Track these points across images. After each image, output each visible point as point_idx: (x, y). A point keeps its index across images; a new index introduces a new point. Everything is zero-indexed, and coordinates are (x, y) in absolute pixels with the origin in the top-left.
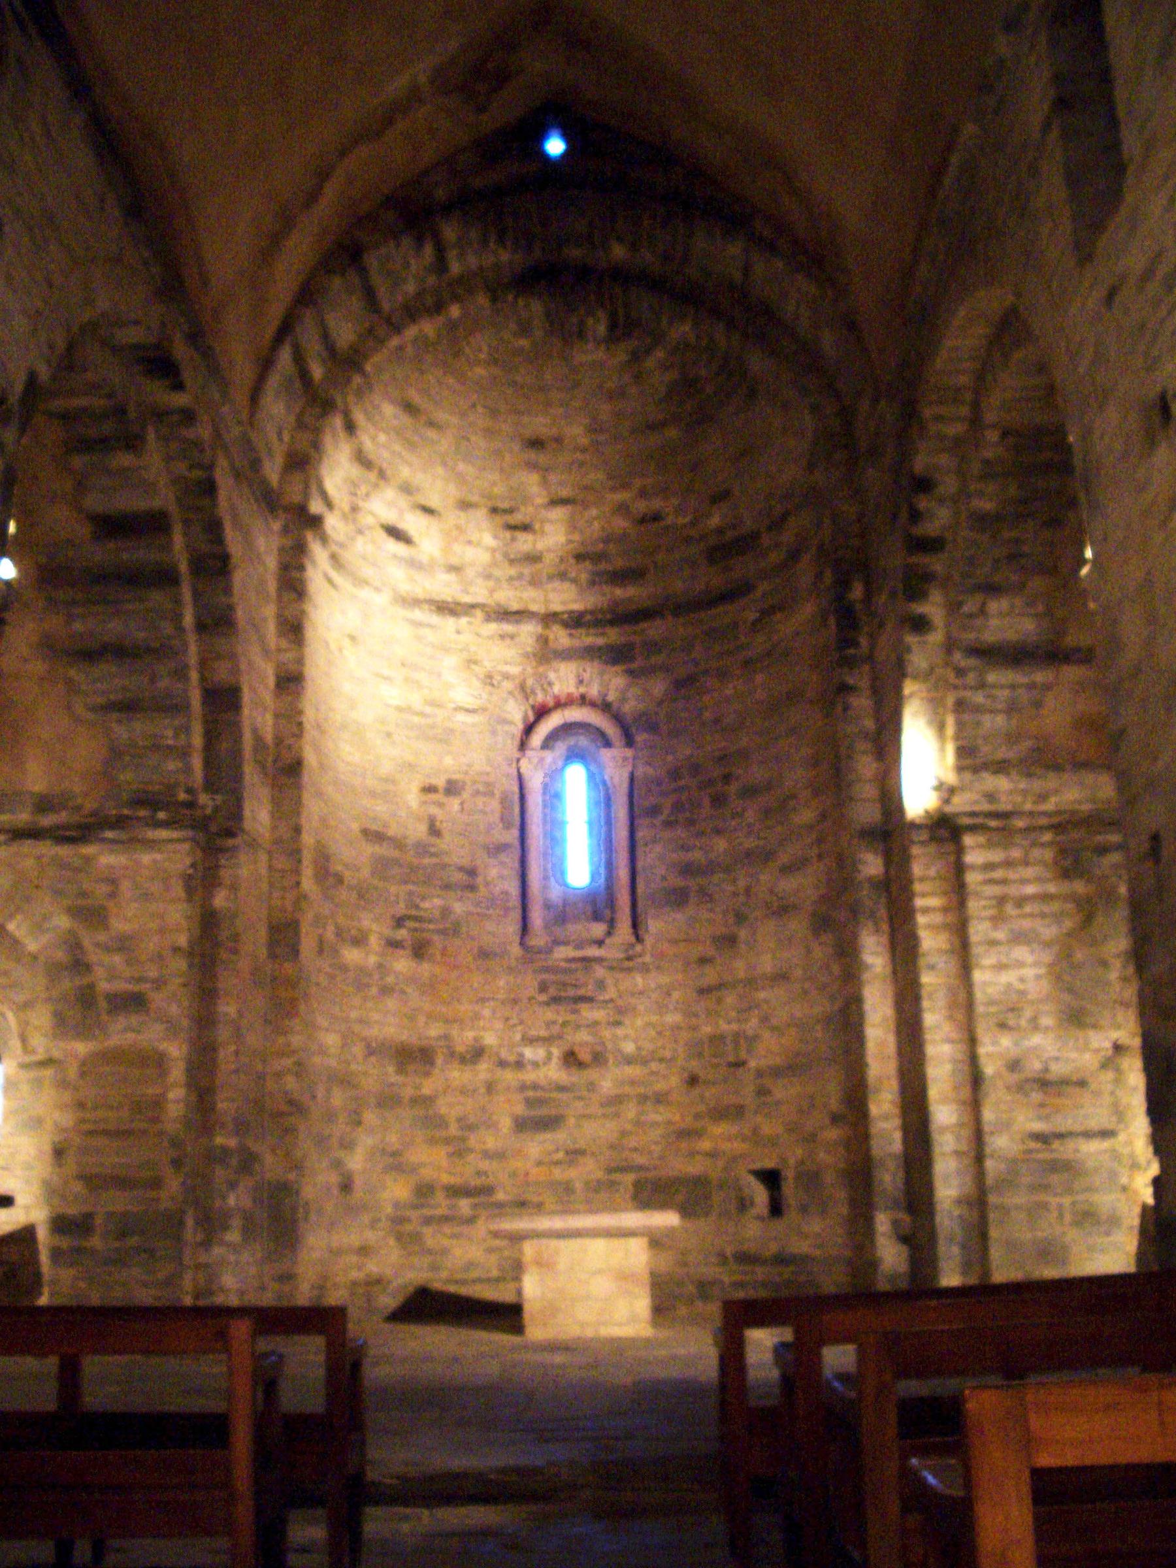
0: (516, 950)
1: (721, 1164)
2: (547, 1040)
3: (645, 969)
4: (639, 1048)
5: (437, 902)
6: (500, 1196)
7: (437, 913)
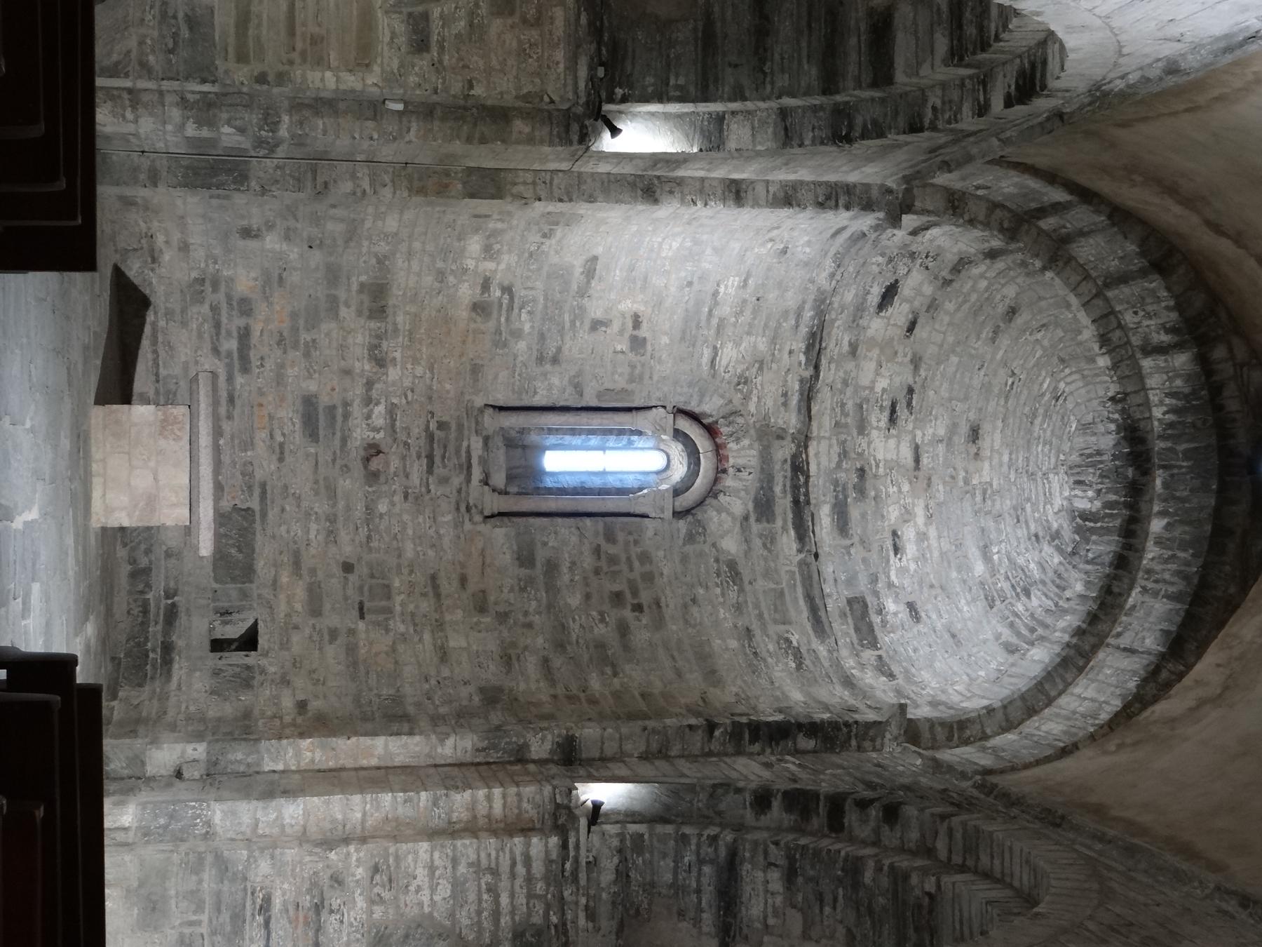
0: (479, 401)
1: (267, 593)
3: (458, 524)
4: (381, 516)
5: (527, 327)
6: (240, 380)
7: (517, 325)
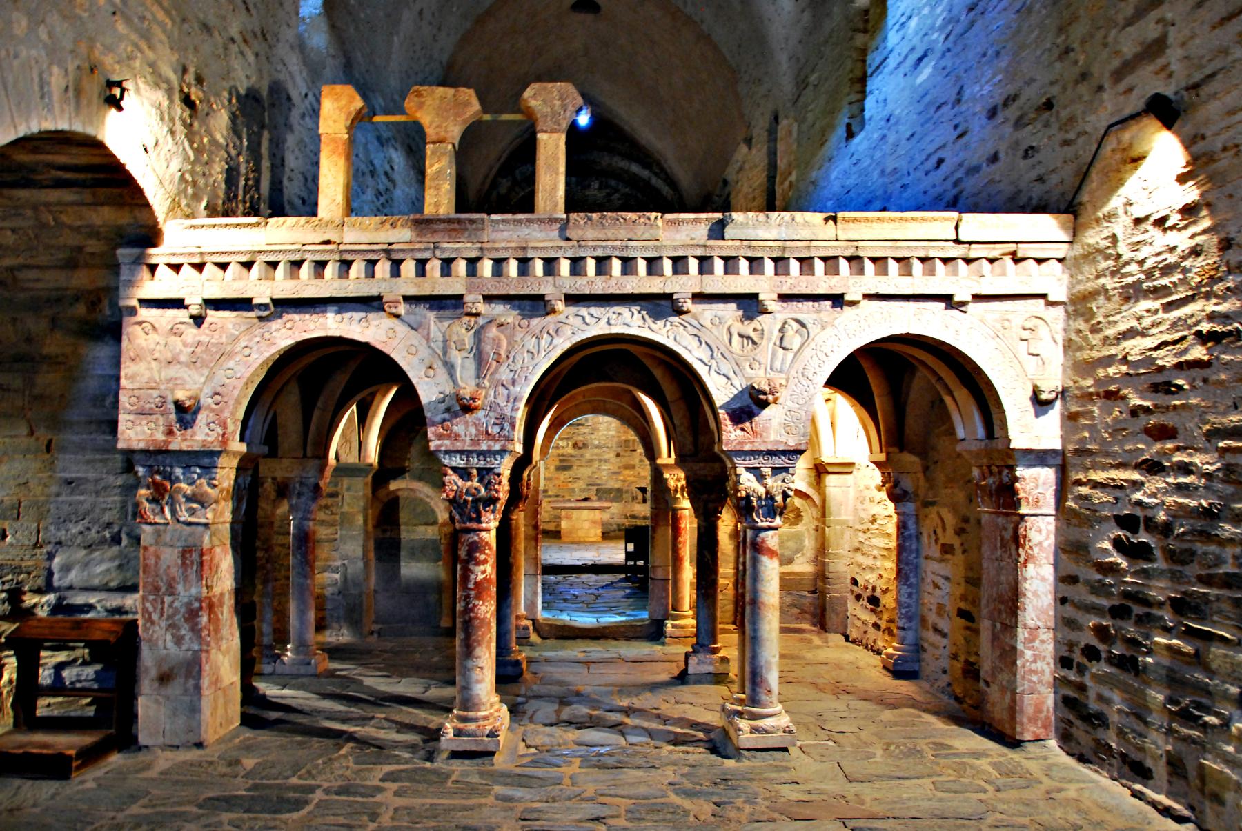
2: (567, 439)
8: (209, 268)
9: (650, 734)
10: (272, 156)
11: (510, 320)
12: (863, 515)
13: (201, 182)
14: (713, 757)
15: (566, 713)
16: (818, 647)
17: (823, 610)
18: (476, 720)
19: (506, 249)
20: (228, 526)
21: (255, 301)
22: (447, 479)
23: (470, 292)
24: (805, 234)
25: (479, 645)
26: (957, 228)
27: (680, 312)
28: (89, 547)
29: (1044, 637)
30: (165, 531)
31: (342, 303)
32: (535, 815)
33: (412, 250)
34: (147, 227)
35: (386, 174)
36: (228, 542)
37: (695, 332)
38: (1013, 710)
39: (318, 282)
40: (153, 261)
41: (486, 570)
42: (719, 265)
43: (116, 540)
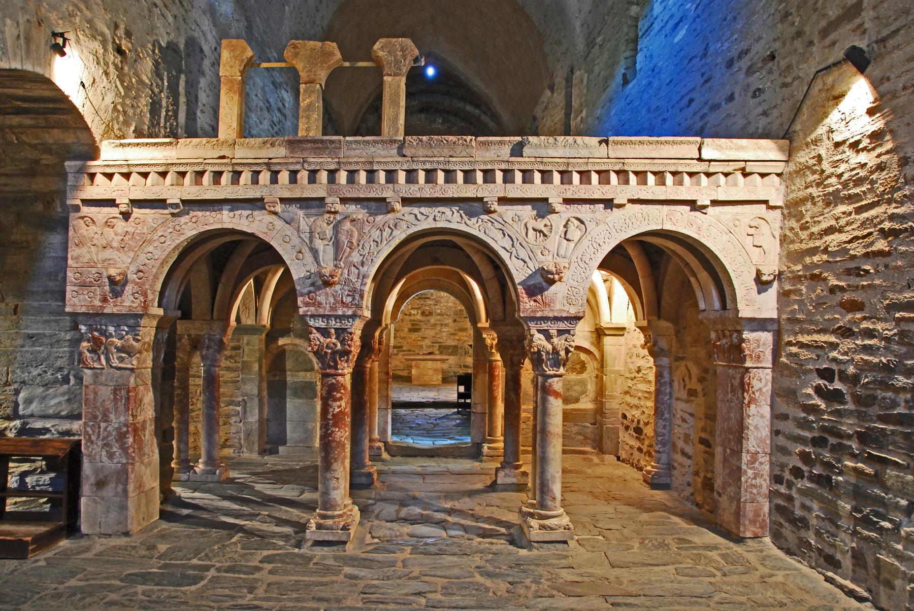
2: (418, 309)
8: (134, 177)
9: (465, 529)
10: (188, 93)
11: (360, 217)
12: (631, 366)
13: (130, 112)
14: (511, 547)
15: (404, 512)
16: (597, 465)
17: (601, 437)
18: (333, 517)
19: (357, 163)
20: (150, 370)
21: (168, 202)
22: (312, 336)
23: (330, 195)
24: (584, 153)
25: (336, 461)
26: (700, 149)
27: (489, 212)
28: (46, 385)
29: (761, 460)
30: (101, 374)
31: (235, 204)
32: (373, 590)
33: (287, 163)
34: (88, 145)
35: (279, 110)
36: (150, 383)
37: (500, 226)
38: (738, 514)
39: (216, 187)
40: (93, 171)
41: (343, 404)
42: (518, 176)
43: (66, 380)
